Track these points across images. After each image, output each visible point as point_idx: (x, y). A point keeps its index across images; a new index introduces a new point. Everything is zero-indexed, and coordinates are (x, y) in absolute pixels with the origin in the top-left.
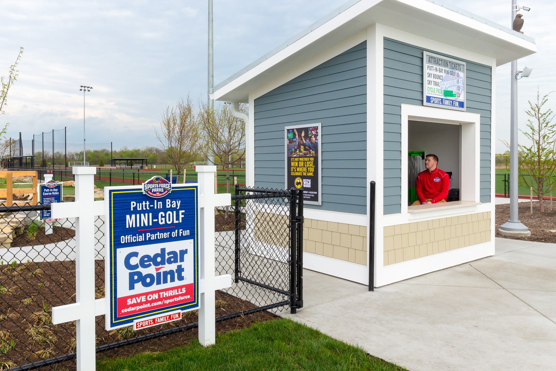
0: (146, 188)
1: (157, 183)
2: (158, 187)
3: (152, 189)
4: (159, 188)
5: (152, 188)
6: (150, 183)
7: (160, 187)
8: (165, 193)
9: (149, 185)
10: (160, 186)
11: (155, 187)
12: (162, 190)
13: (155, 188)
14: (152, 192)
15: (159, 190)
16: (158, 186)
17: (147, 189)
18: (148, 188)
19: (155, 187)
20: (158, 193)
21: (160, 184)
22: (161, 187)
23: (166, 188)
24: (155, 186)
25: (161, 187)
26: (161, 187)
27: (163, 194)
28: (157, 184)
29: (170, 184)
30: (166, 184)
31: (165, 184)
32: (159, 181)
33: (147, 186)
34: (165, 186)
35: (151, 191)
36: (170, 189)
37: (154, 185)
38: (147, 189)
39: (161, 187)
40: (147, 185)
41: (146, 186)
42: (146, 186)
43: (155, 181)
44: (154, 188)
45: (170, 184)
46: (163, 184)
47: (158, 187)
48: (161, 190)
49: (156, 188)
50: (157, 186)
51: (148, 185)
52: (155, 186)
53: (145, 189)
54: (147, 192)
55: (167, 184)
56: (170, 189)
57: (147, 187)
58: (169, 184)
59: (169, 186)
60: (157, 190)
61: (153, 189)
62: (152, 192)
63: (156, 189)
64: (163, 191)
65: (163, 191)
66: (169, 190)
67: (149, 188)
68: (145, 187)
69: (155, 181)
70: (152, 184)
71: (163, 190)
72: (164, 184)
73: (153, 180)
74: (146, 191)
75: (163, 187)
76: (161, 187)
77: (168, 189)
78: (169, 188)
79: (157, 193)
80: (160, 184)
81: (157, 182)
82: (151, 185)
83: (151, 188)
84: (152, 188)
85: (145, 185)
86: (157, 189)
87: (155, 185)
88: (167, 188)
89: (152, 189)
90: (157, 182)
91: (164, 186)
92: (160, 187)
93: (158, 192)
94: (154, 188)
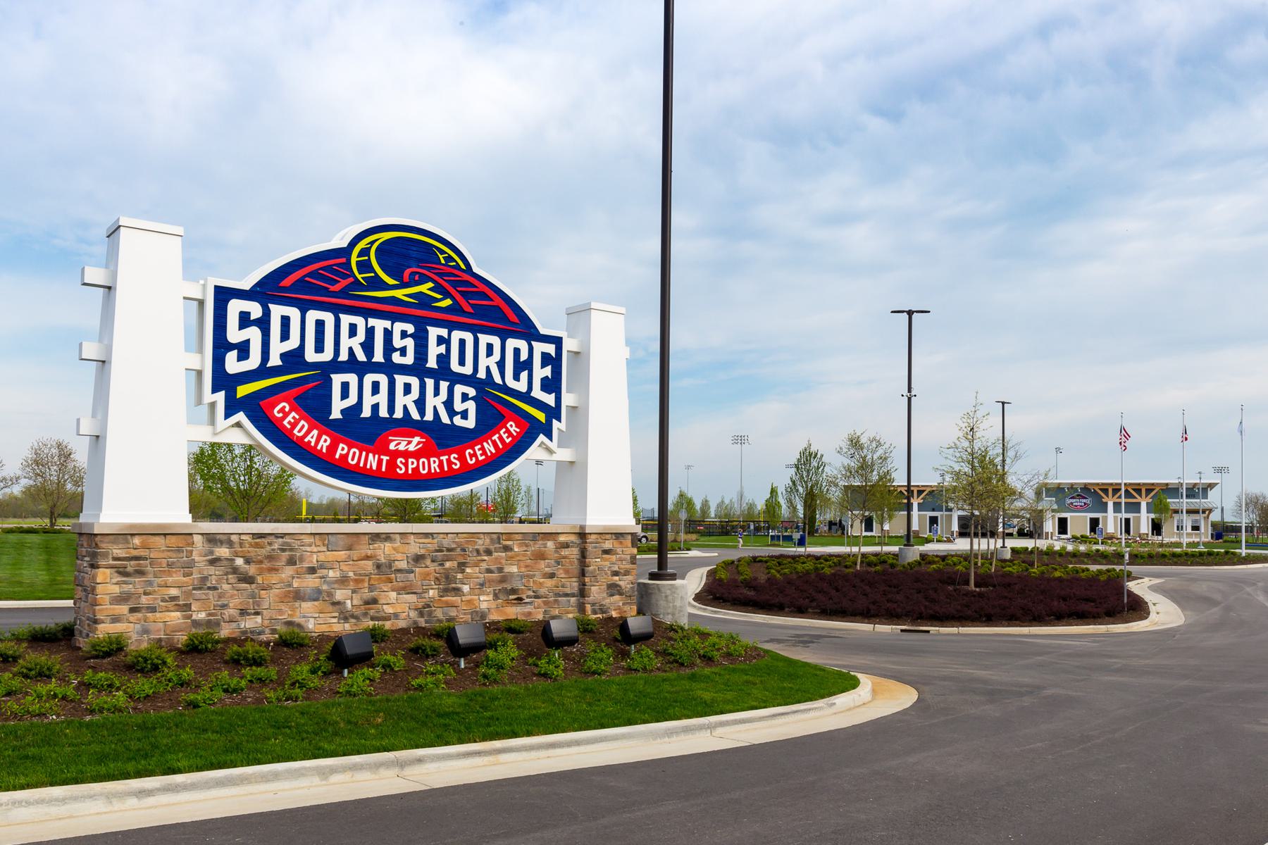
0: (243, 350)
1: (393, 312)
2: (409, 359)
3: (337, 379)
4: (419, 369)
5: (327, 356)
6: (301, 285)
7: (432, 363)
8: (490, 448)
9: (294, 313)
10: (434, 351)
11: (378, 357)
12: (458, 406)
13: (371, 367)
14: (336, 414)
15: (420, 404)
16: (410, 343)
17: (253, 362)
18: (275, 361)
19: (378, 357)
20: (415, 443)
21: (434, 332)
22: (443, 372)
23: (511, 383)
24: (368, 346)
25: (443, 372)
26: (444, 359)
27: (477, 454)
28: (395, 318)
29: (550, 349)
30: (512, 343)
31: (496, 341)
32: (425, 288)
33: (264, 324)
34: (492, 362)
35: (314, 404)
36: (549, 399)
37: (359, 321)
38: (263, 371)
39: (444, 359)
40: (255, 310)
41: (245, 321)
42: (245, 321)
43: (377, 284)
44: (351, 365)
45: (550, 349)
46: (475, 330)
47: (409, 359)
48: (449, 404)
49: (390, 369)
50: (397, 342)
51: (277, 311)
52: (368, 346)
53: (233, 364)
54: (257, 409)
55: (522, 345)
56: (549, 399)
57: (254, 334)
58: (539, 348)
59: (541, 372)
60: (401, 400)
61: (352, 378)
62: (336, 414)
63: (383, 379)
64: (470, 423)
65: (470, 423)
66: (541, 416)
67: (294, 359)
68: (234, 334)
69: (377, 284)
70: (337, 310)
71: (471, 406)
72: (484, 339)
73: (345, 252)
74: (243, 391)
75: (468, 370)
76: (455, 366)
77: (527, 397)
78: (537, 393)
79: (399, 444)
80: (434, 332)
81: (399, 294)
82: (313, 316)
83: (311, 356)
84: (335, 366)
85: (235, 307)
86: (400, 380)
87: (380, 325)
88: (521, 386)
89: (337, 379)
90: (399, 294)
91: (484, 362)
92: (432, 363)
93: (407, 426)
94: (351, 365)
